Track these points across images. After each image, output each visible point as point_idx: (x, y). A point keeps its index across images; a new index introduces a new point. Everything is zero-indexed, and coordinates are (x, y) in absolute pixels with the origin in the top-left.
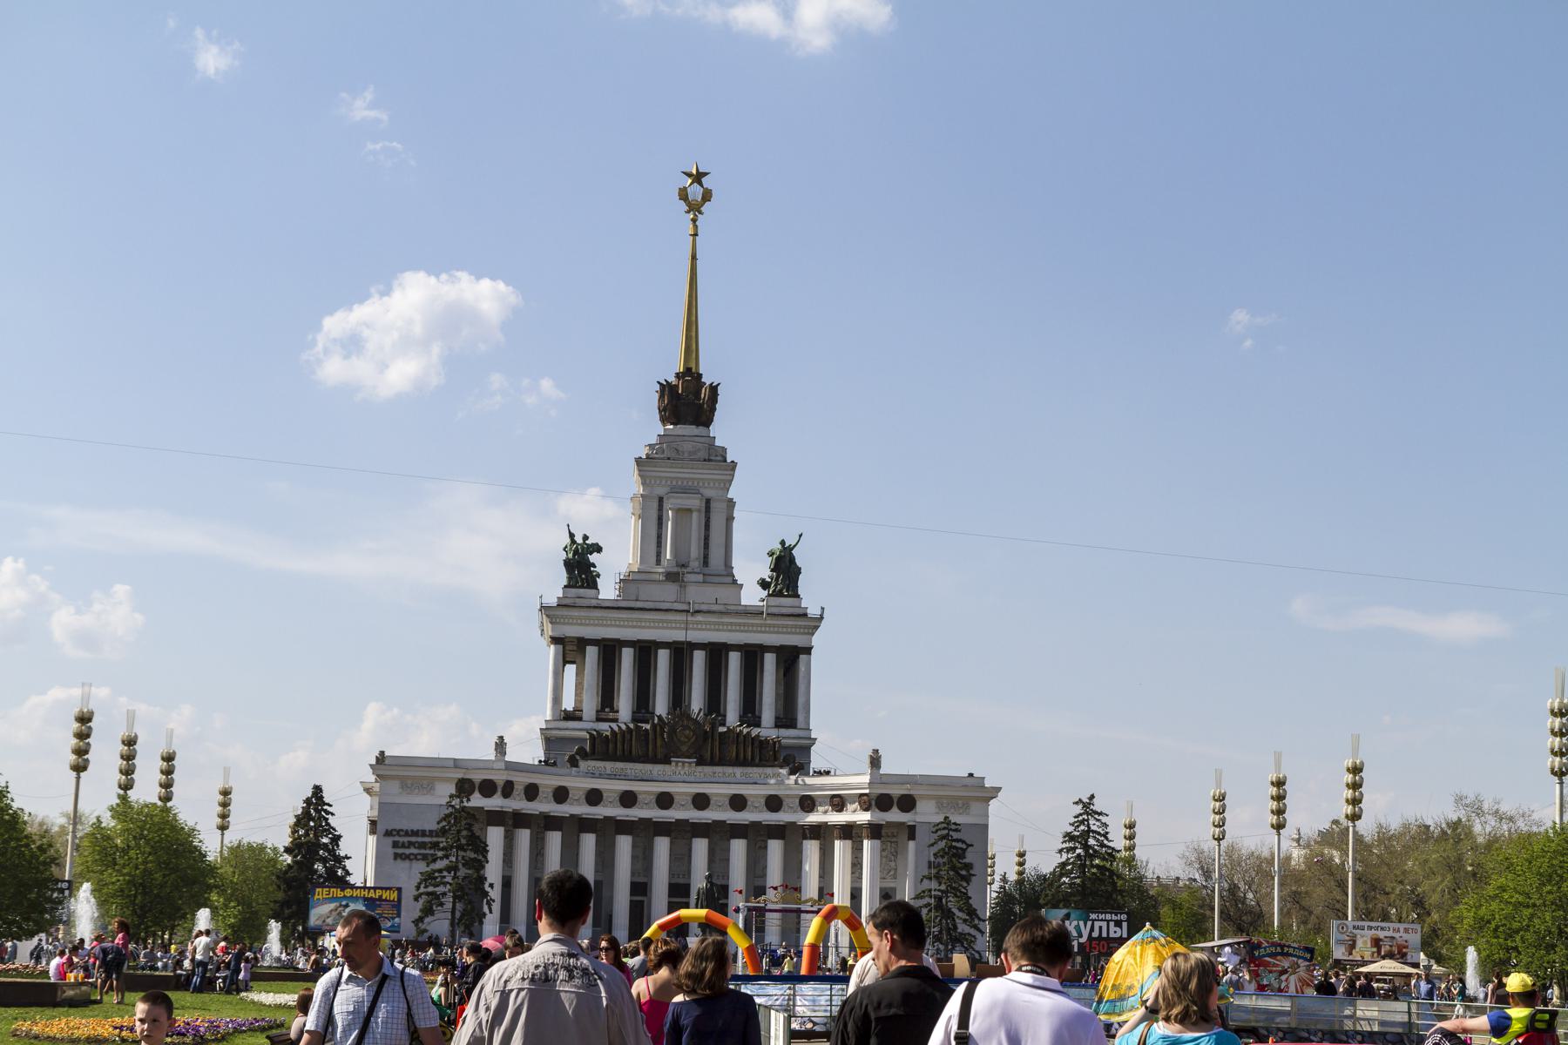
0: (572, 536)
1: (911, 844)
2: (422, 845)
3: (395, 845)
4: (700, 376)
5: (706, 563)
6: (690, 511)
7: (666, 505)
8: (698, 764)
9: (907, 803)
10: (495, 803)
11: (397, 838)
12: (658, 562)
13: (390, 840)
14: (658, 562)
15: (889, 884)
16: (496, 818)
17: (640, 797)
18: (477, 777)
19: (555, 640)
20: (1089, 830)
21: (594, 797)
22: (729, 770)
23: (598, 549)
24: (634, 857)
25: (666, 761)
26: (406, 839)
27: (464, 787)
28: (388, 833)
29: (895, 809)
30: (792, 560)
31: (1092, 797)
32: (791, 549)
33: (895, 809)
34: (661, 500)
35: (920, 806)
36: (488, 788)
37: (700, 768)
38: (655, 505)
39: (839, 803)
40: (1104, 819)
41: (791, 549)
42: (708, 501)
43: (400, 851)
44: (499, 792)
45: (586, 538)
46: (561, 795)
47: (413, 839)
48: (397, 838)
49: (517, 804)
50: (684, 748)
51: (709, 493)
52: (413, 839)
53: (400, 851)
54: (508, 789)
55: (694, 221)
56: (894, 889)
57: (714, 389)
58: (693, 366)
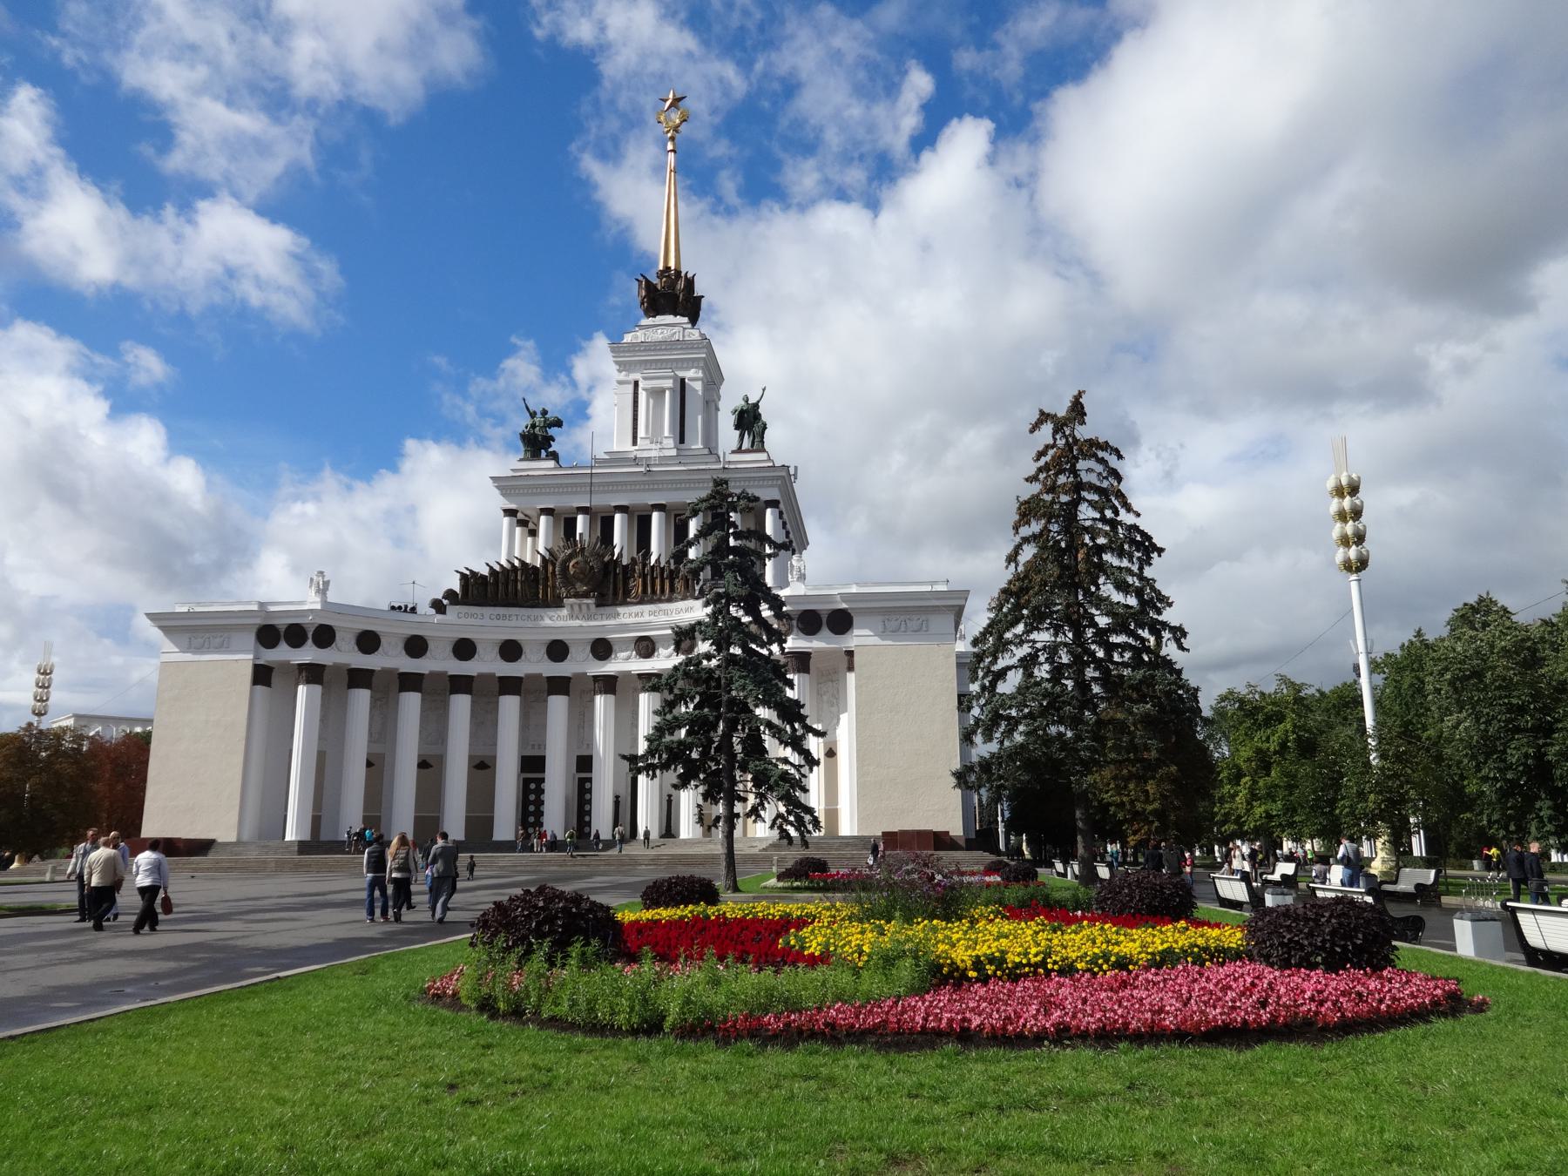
0: (533, 415)
1: (851, 677)
4: (678, 272)
5: (682, 441)
6: (661, 392)
7: (641, 385)
8: (598, 605)
9: (841, 622)
10: (308, 654)
12: (635, 443)
14: (635, 443)
16: (313, 674)
17: (526, 649)
18: (281, 623)
19: (510, 513)
20: (1079, 486)
21: (465, 649)
23: (558, 423)
24: (543, 727)
25: (557, 603)
27: (268, 635)
29: (825, 632)
30: (757, 417)
31: (1078, 410)
32: (756, 405)
33: (825, 632)
34: (636, 384)
36: (295, 635)
37: (602, 610)
38: (631, 387)
40: (1113, 461)
41: (756, 405)
42: (683, 380)
44: (310, 642)
45: (545, 412)
46: (416, 646)
49: (343, 654)
51: (681, 374)
54: (325, 636)
55: (672, 139)
57: (690, 283)
58: (672, 264)
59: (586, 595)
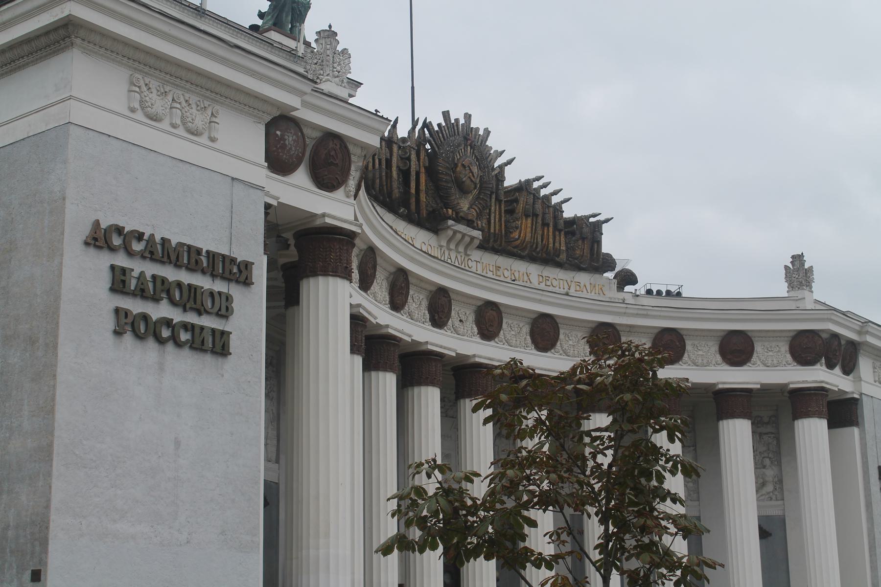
2: (191, 299)
3: (119, 282)
11: (121, 260)
13: (104, 261)
15: (773, 511)
22: (521, 267)
25: (432, 222)
26: (151, 269)
28: (100, 239)
35: (865, 365)
39: (736, 348)
43: (136, 306)
47: (171, 274)
48: (121, 260)
50: (464, 205)
52: (171, 274)
53: (136, 306)
56: (782, 521)
59: (470, 223)
